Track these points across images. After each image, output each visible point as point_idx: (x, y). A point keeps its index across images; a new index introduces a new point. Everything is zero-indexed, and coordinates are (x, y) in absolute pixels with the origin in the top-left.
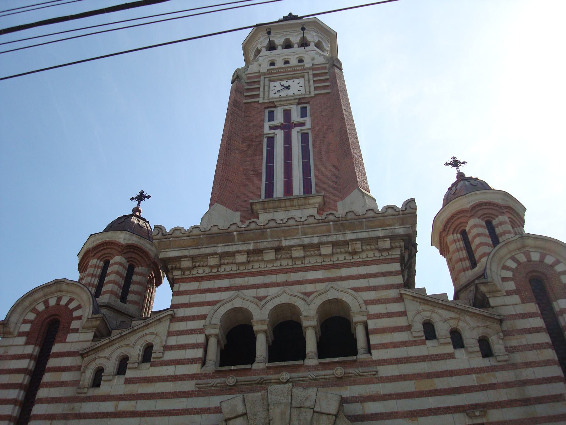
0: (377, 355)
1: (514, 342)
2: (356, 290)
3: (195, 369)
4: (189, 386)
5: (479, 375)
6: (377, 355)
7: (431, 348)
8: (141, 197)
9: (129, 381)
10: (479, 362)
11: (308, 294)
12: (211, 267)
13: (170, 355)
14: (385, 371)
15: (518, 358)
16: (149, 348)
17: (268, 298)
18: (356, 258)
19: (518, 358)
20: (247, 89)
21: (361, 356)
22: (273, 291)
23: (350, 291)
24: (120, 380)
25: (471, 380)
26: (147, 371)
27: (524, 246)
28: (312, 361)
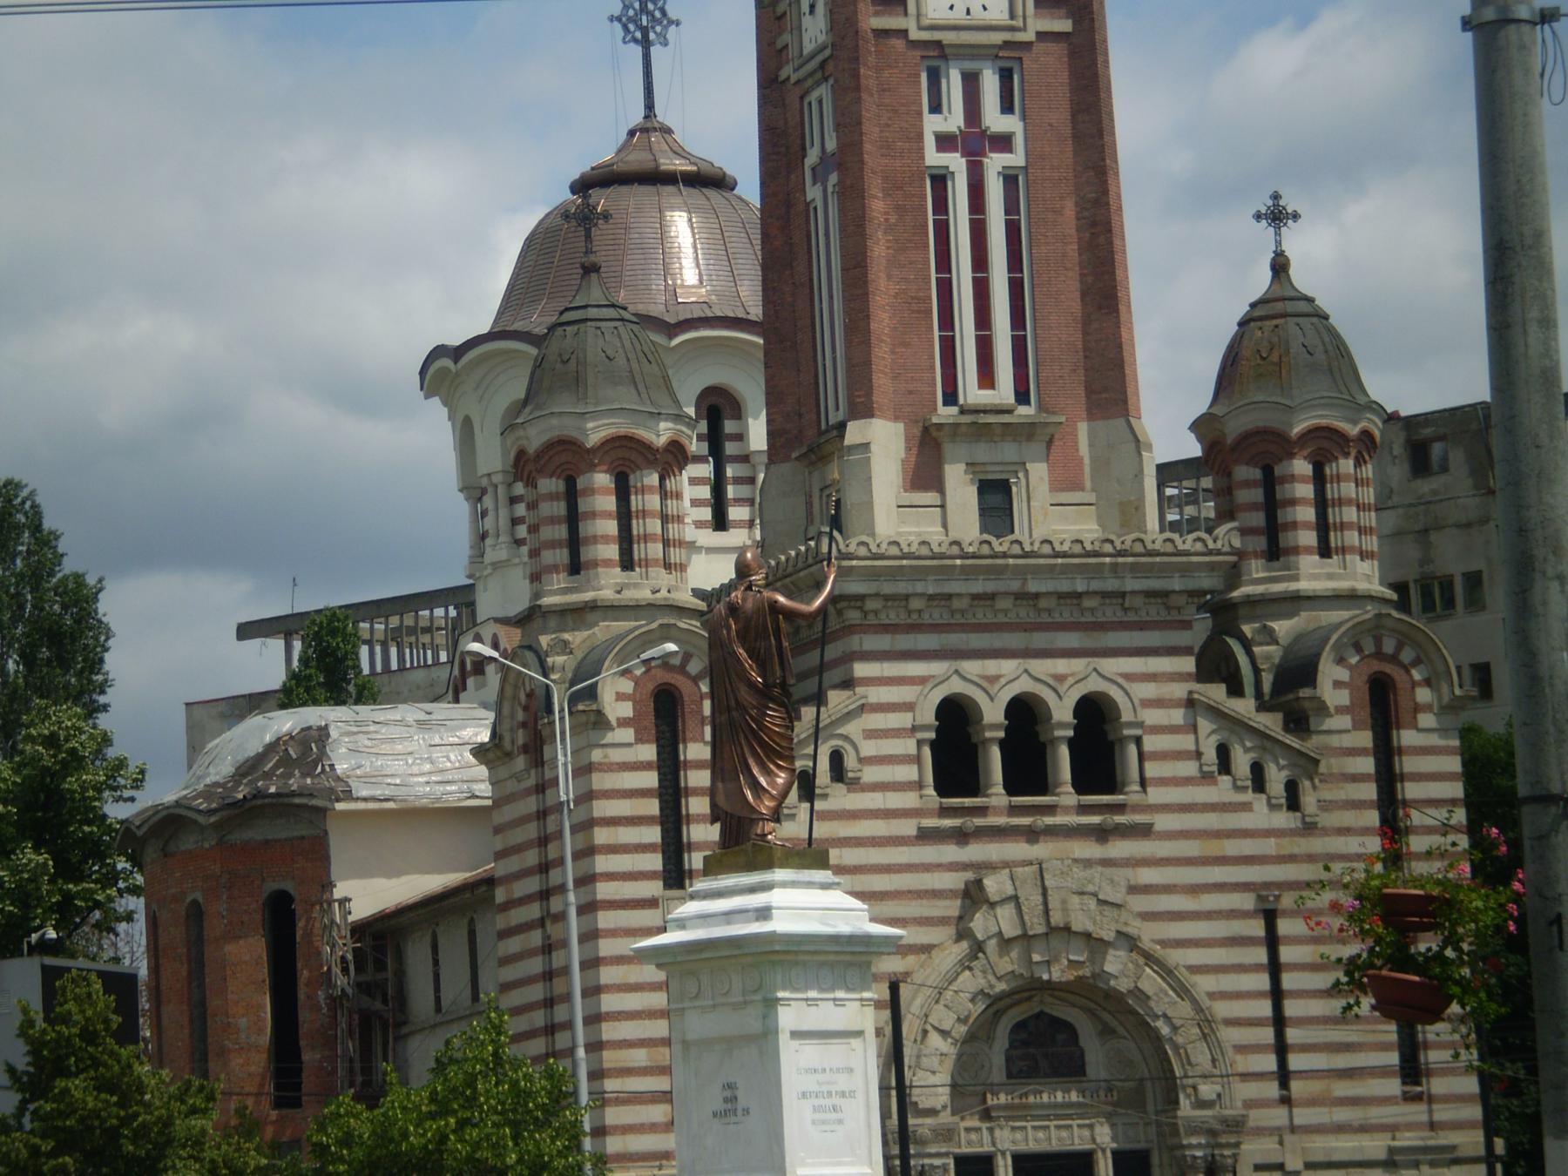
0: (1155, 795)
2: (1130, 677)
3: (909, 800)
4: (908, 827)
6: (1155, 795)
7: (1222, 789)
10: (1283, 819)
11: (1061, 678)
13: (870, 774)
14: (1163, 822)
16: (837, 758)
17: (1003, 681)
21: (1132, 796)
22: (1008, 666)
25: (1269, 846)
26: (838, 798)
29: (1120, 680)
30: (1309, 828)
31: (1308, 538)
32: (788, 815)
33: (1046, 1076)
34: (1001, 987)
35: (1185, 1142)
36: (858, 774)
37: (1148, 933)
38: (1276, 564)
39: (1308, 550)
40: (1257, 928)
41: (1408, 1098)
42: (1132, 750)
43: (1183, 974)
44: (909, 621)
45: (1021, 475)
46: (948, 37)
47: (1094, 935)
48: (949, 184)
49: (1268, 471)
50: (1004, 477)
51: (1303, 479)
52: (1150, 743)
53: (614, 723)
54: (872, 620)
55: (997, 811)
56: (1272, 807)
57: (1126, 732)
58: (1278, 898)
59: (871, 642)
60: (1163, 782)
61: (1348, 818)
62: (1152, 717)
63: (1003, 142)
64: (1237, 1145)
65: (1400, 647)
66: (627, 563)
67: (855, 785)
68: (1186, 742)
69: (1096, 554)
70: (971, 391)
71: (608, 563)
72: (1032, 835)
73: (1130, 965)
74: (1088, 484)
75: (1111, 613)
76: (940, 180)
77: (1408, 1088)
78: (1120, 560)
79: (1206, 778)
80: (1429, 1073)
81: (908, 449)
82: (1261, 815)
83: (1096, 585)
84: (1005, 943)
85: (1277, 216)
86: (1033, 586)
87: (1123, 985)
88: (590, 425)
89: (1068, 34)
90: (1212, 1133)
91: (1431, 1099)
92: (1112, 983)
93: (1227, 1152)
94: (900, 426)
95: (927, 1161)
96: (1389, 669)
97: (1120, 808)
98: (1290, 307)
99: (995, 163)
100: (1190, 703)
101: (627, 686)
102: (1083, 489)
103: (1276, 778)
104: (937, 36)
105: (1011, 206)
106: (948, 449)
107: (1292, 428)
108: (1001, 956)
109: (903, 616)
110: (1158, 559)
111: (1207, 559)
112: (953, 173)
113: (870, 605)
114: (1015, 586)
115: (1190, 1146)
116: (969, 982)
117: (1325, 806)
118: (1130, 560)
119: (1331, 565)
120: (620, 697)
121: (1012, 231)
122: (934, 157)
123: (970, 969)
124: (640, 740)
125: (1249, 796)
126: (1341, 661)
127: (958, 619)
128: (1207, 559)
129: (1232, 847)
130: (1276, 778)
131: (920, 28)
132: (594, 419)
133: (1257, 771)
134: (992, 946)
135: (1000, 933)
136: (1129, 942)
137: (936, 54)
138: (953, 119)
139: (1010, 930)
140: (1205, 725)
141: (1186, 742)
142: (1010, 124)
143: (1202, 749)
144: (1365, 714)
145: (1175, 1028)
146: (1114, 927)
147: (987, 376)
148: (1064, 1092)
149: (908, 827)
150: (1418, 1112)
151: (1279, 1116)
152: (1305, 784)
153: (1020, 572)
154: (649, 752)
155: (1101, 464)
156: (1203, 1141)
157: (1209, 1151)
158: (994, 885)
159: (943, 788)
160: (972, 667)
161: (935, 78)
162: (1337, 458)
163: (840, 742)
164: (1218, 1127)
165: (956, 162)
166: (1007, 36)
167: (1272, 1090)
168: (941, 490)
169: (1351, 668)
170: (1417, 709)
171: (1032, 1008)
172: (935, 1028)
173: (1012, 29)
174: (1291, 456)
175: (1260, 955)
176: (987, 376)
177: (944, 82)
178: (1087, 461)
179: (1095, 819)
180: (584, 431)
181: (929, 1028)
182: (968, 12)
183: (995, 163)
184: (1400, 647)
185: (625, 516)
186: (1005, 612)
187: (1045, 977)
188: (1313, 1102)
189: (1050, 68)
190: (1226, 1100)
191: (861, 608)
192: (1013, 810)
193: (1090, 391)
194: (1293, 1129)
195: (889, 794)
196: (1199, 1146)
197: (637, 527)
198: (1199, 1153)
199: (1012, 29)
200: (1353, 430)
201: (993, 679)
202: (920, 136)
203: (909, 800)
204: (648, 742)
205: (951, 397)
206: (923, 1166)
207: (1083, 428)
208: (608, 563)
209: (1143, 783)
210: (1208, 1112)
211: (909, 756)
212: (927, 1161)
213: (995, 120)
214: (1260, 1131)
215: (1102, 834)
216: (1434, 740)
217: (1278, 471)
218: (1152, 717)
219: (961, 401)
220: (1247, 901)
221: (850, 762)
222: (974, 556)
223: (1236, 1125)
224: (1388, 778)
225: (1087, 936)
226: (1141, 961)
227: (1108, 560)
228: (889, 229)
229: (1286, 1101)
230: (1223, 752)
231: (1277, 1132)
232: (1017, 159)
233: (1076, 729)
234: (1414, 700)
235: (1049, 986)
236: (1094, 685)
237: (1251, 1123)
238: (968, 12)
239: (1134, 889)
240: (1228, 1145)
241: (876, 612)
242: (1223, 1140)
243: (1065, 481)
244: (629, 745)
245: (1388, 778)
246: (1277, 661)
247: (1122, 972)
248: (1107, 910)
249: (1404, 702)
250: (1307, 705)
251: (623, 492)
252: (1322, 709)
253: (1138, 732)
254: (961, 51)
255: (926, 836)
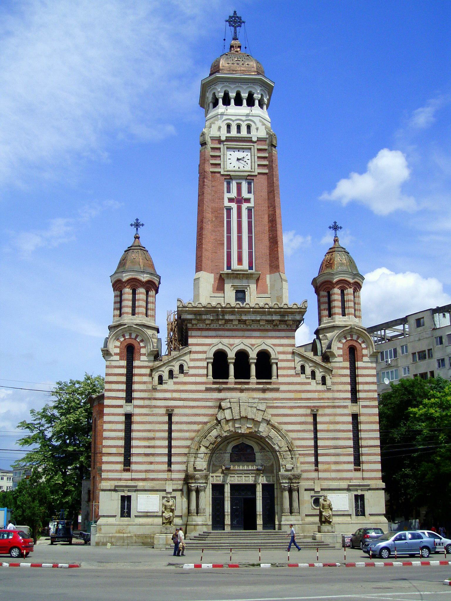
0: (281, 380)
1: (336, 380)
2: (275, 345)
3: (204, 379)
4: (203, 387)
5: (319, 393)
6: (281, 380)
7: (302, 378)
8: (137, 225)
9: (175, 383)
10: (321, 387)
11: (253, 345)
12: (207, 324)
13: (192, 372)
14: (282, 388)
15: (335, 388)
16: (181, 367)
17: (235, 345)
18: (276, 327)
19: (335, 388)
20: (212, 156)
21: (274, 379)
22: (237, 341)
23: (272, 346)
24: (171, 382)
25: (316, 395)
26: (182, 378)
27: (351, 332)
28: (253, 379)
29: (272, 346)
30: (329, 390)
31: (339, 311)
32: (165, 383)
33: (244, 461)
34: (225, 434)
35: (281, 482)
36: (188, 371)
37: (274, 421)
38: (330, 318)
39: (338, 314)
40: (310, 419)
41: (356, 470)
42: (274, 367)
43: (283, 432)
44: (207, 327)
45: (248, 288)
46: (231, 173)
47: (255, 419)
48: (232, 210)
49: (329, 293)
50: (243, 289)
51: (337, 294)
52: (280, 364)
53: (113, 354)
54: (195, 327)
55: (231, 383)
56: (317, 384)
57: (273, 361)
58: (317, 410)
59: (194, 333)
60: (284, 376)
61: (340, 387)
62: (281, 357)
63: (248, 200)
64: (299, 483)
65: (358, 338)
66: (133, 314)
67: (186, 374)
68: (292, 364)
69: (263, 308)
70: (235, 265)
71: (127, 313)
72: (242, 391)
73: (267, 429)
74: (269, 292)
75: (269, 327)
76: (229, 210)
77: (355, 467)
78: (271, 310)
79: (297, 375)
80: (363, 463)
81: (215, 281)
82: (314, 385)
83: (264, 318)
84: (227, 421)
85: (335, 228)
86: (244, 318)
87: (264, 434)
88: (124, 275)
89: (267, 173)
90: (290, 479)
91: (363, 471)
92: (261, 434)
93: (295, 485)
94: (213, 275)
95: (198, 485)
96: (355, 344)
97: (270, 383)
98: (336, 249)
99: (245, 206)
100: (293, 353)
101: (118, 344)
102: (267, 293)
103: (319, 376)
104: (229, 173)
105: (250, 217)
106: (226, 281)
107: (333, 279)
108: (226, 425)
109: (205, 326)
110: (282, 310)
111: (298, 310)
112: (232, 208)
113: (194, 322)
114: (238, 317)
115: (283, 483)
116: (214, 433)
117: (333, 384)
118: (273, 310)
119: (345, 318)
120: (116, 347)
121: (250, 224)
122: (227, 203)
123: (216, 429)
124: (121, 359)
125: (310, 380)
126: (340, 341)
127: (222, 327)
128: (298, 310)
129: (304, 395)
130: (319, 376)
131: (224, 171)
132: (125, 273)
133: (313, 373)
134: (223, 422)
135: (225, 418)
136: (268, 422)
137: (229, 178)
138: (234, 194)
139: (229, 417)
140: (297, 359)
141: (292, 364)
142: (251, 196)
143: (296, 366)
144: (347, 357)
145: (280, 448)
146: (261, 417)
147: (240, 261)
148: (242, 466)
149: (203, 387)
150: (358, 474)
151: (314, 475)
152: (328, 378)
153: (240, 313)
154: (124, 363)
155: (272, 286)
156: (287, 482)
157: (289, 484)
158: (223, 404)
159: (215, 376)
160: (226, 341)
161: (229, 184)
162: (347, 288)
163: (182, 362)
164: (292, 477)
165: (234, 206)
166: (249, 173)
167: (313, 467)
168: (224, 293)
169: (343, 344)
170: (363, 356)
171: (240, 441)
172: (203, 446)
173: (251, 172)
174: (334, 287)
175: (311, 427)
176: (240, 261)
177: (231, 184)
178: (269, 285)
179: (261, 386)
180: (122, 277)
181: (201, 445)
182: (239, 168)
183: (245, 206)
184: (358, 339)
185: (134, 300)
186: (237, 325)
187: (240, 432)
188: (325, 471)
189: (262, 183)
190: (295, 469)
191: (191, 323)
192: (236, 383)
193: (271, 266)
194: (319, 479)
195: (197, 377)
196: (286, 483)
197: (137, 304)
198: (286, 485)
199: (251, 172)
200: (351, 281)
201: (232, 345)
202: (223, 199)
203: (204, 379)
204: (123, 360)
205: (229, 267)
206: (197, 486)
207: (268, 277)
208: (127, 313)
209: (277, 377)
210: (290, 473)
211: (204, 366)
212: (198, 485)
213: (245, 194)
214: (308, 479)
215: (264, 391)
216: (370, 365)
217: (331, 293)
218: (281, 357)
219: (232, 268)
220: (308, 411)
221: (185, 368)
222: (225, 308)
223: (298, 477)
224: (354, 376)
225: (253, 420)
226: (270, 427)
227: (266, 310)
228: (212, 222)
229: (317, 470)
230: (303, 368)
231: (313, 479)
232: (252, 204)
233: (257, 360)
234: (362, 353)
235: (243, 435)
236: (264, 347)
237: (302, 477)
238: (239, 168)
239: (269, 407)
240: (295, 483)
241: (196, 325)
242: (294, 481)
243: (261, 290)
244: (118, 361)
245: (354, 376)
246: (327, 344)
247: (264, 431)
248: (260, 412)
249: (359, 354)
250: (328, 354)
251: (134, 293)
252: (333, 355)
253: (277, 361)
254: (236, 177)
255: (208, 390)
